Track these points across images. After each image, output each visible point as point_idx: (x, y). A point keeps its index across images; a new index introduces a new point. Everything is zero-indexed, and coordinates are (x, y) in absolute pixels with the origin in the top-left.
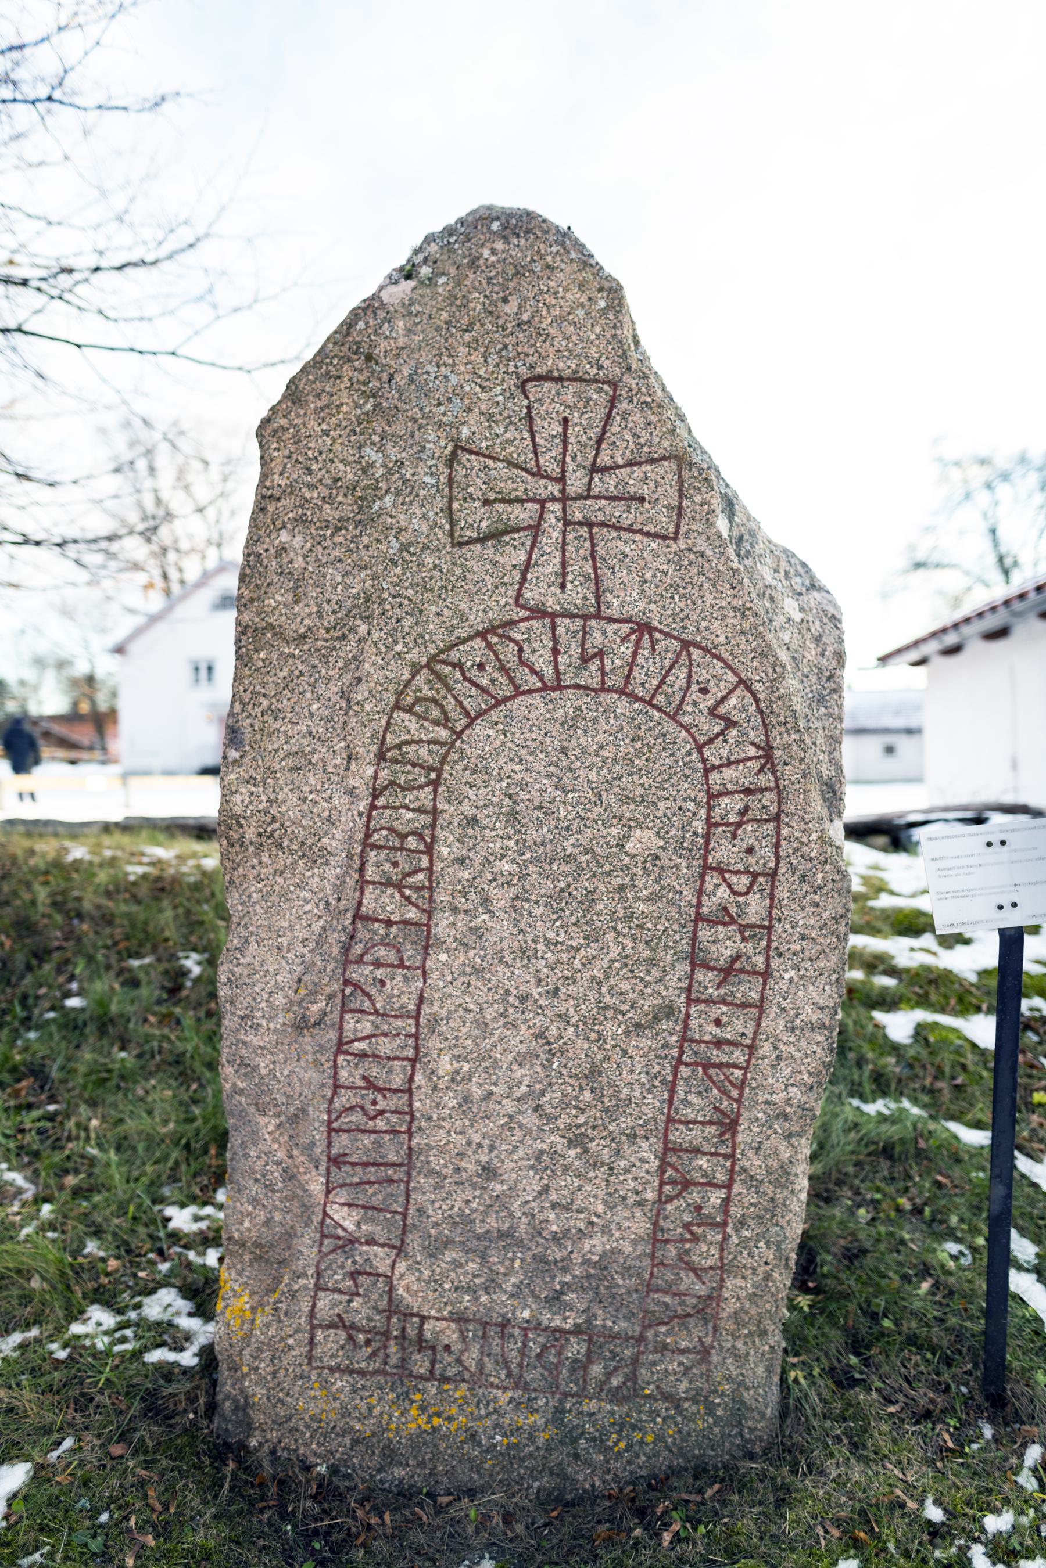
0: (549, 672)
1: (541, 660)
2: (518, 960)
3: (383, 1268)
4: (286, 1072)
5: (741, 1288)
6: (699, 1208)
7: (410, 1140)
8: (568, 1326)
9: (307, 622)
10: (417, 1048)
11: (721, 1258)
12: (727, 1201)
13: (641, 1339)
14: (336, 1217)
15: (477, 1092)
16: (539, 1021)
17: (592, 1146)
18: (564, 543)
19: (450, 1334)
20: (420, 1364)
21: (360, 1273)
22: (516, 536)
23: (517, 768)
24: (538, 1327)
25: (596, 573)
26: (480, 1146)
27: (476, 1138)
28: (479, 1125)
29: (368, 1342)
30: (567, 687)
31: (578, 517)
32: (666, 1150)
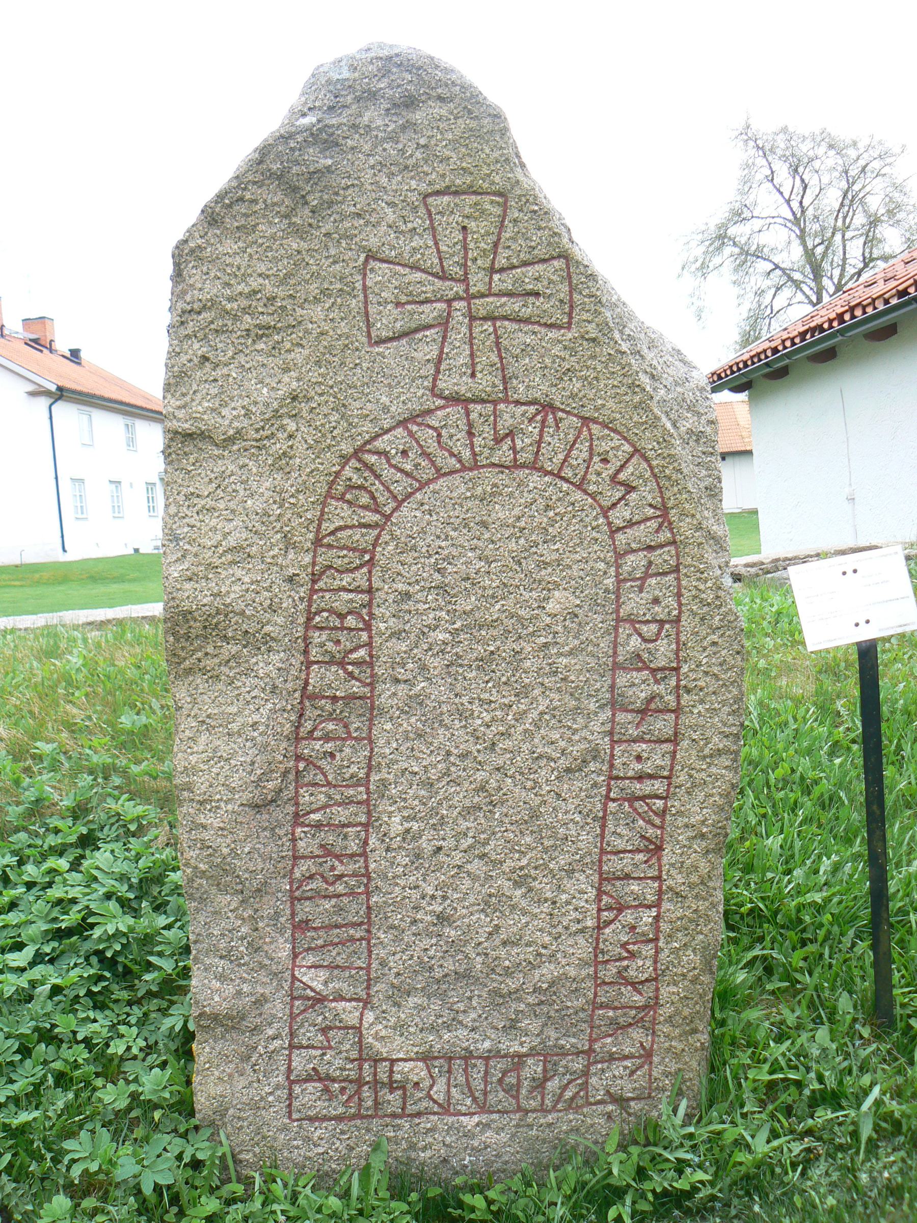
0: (466, 454)
1: (459, 443)
2: (456, 722)
3: (352, 1019)
4: (247, 850)
5: (674, 993)
6: (633, 928)
7: (368, 900)
8: (524, 1050)
9: (236, 424)
10: (369, 813)
11: (655, 970)
12: (657, 918)
13: (591, 1050)
14: (304, 979)
15: (428, 848)
16: (480, 776)
17: (535, 884)
18: (471, 338)
19: (416, 1071)
20: (393, 1099)
21: (330, 1028)
22: (428, 333)
23: (443, 544)
24: (498, 1054)
25: (502, 362)
26: (433, 897)
27: (430, 891)
28: (431, 878)
29: (343, 1090)
30: (483, 466)
31: (482, 313)
32: (602, 879)
